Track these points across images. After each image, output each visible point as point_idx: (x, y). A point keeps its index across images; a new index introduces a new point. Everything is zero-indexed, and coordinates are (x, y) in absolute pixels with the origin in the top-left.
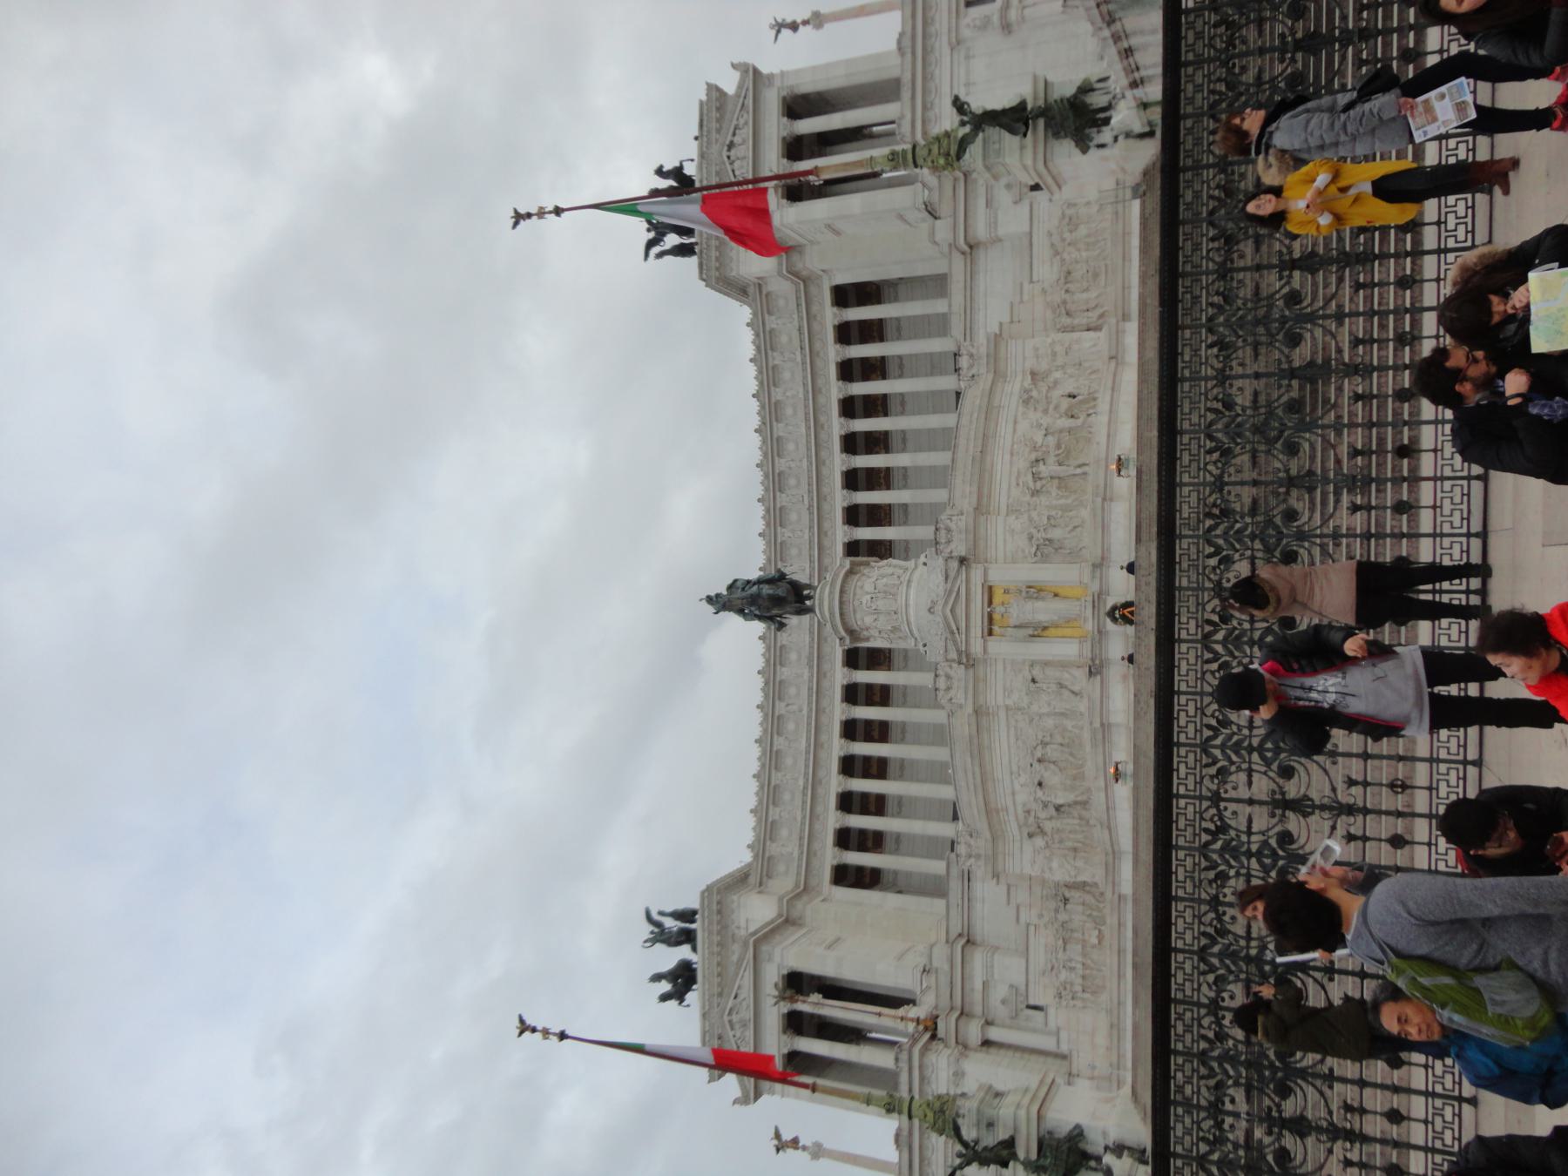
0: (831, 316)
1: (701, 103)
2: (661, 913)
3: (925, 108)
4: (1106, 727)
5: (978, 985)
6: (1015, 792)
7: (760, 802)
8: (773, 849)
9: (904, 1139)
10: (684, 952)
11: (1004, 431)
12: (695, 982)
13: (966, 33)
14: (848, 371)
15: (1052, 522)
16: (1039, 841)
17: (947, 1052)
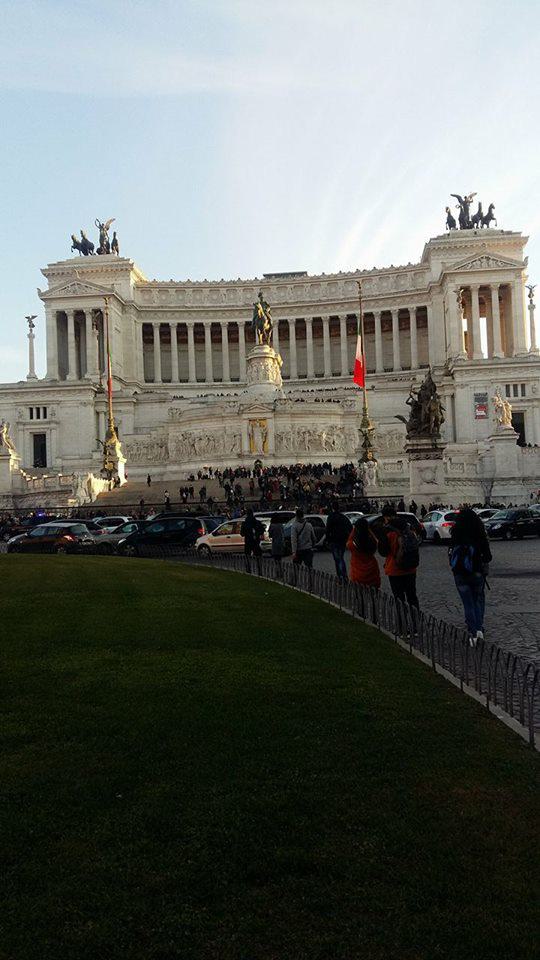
0: (412, 306)
1: (520, 233)
2: (115, 233)
3: (466, 370)
4: (222, 460)
5: (119, 408)
6: (197, 429)
7: (177, 284)
8: (155, 292)
9: (54, 384)
10: (97, 245)
11: (322, 420)
12: (86, 254)
13: (495, 386)
14: (386, 315)
15: (288, 440)
16: (181, 438)
17: (91, 398)
